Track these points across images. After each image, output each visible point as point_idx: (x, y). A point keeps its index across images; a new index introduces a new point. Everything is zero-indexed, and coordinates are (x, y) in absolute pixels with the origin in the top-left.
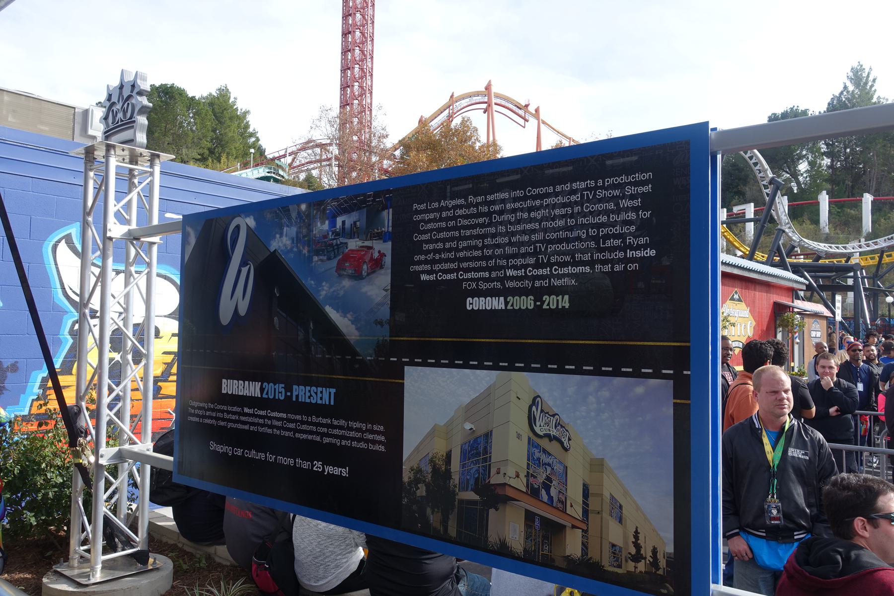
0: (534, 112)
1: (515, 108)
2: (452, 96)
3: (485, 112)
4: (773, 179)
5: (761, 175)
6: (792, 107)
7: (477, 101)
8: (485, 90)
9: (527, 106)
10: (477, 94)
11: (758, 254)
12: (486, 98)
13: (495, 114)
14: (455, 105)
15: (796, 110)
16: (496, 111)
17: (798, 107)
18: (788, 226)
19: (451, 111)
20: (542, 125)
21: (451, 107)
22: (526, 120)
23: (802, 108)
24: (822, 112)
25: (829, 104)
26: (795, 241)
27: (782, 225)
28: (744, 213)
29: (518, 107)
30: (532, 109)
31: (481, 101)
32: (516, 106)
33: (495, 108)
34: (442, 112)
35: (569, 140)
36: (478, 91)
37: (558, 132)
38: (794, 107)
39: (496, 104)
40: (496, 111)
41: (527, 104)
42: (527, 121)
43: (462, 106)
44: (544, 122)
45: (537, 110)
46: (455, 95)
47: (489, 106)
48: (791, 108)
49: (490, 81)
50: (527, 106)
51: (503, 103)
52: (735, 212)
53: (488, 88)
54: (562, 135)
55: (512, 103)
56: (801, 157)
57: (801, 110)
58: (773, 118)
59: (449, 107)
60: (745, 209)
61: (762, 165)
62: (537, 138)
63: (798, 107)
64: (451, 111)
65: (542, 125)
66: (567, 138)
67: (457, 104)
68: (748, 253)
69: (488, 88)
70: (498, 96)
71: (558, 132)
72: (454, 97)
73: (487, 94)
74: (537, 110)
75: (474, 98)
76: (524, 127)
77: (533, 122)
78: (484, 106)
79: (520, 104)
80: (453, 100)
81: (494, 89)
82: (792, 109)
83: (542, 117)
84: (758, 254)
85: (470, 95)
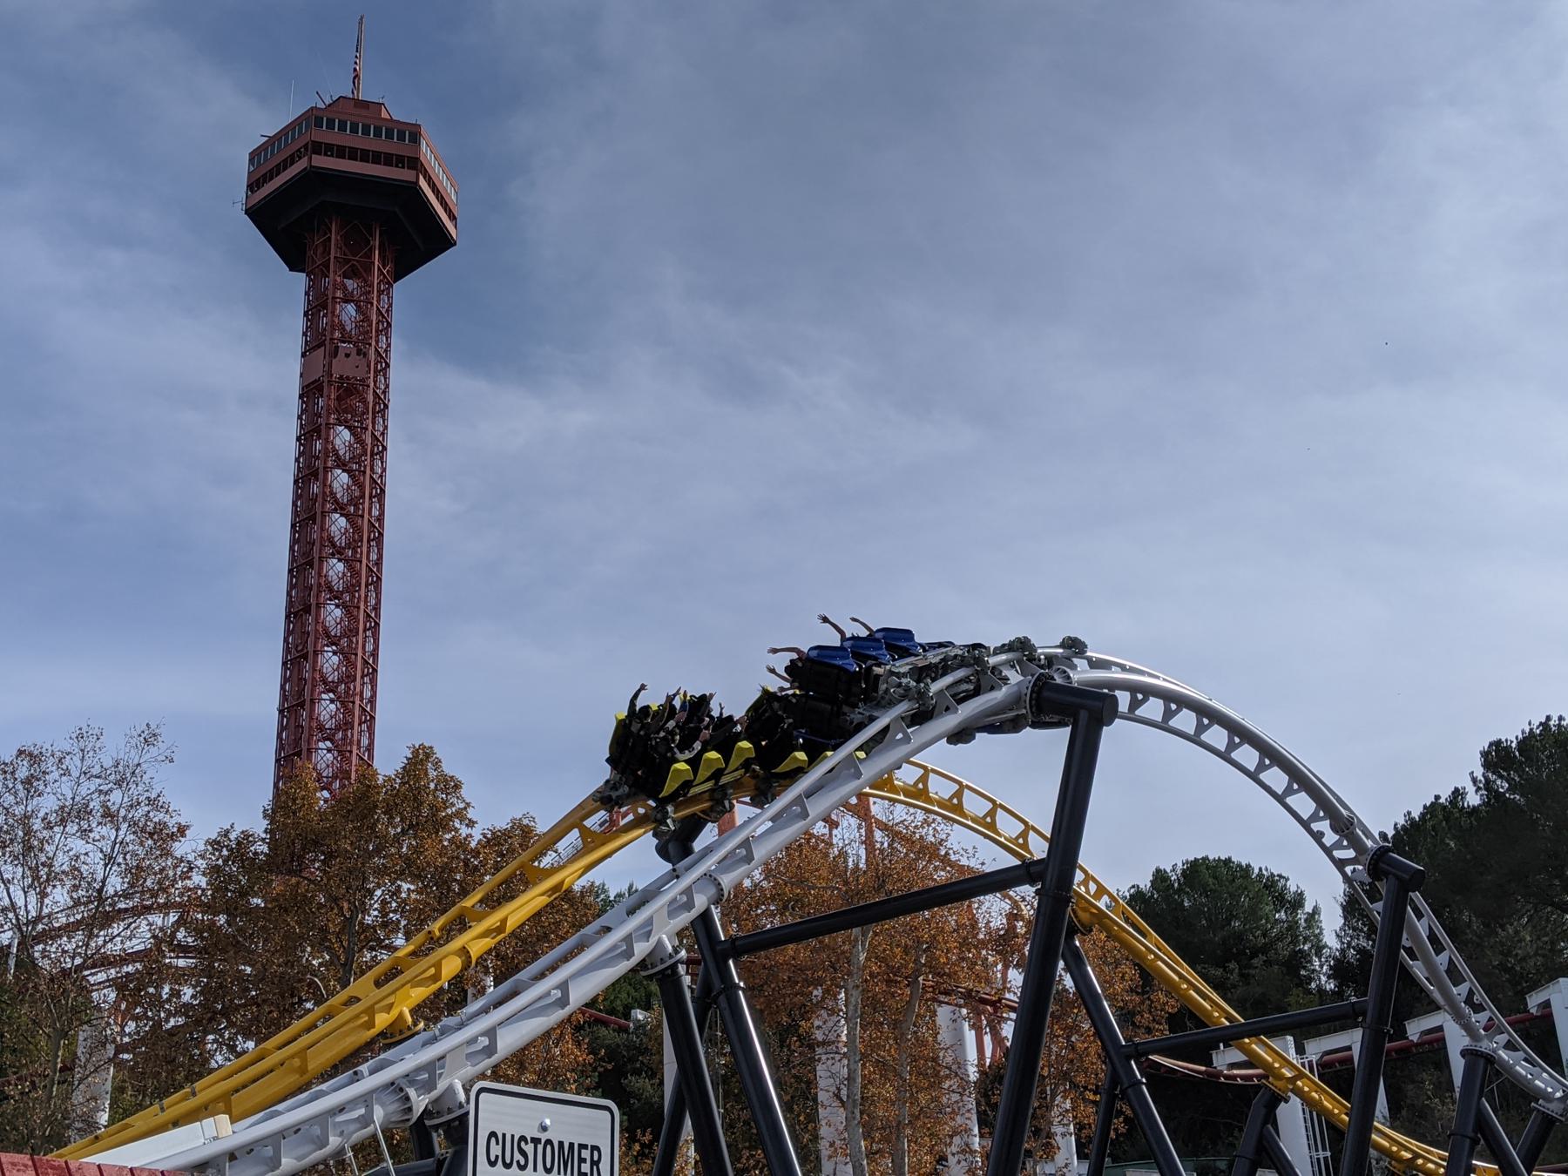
6: (1543, 720)
17: (1561, 718)
18: (1502, 1039)
26: (1548, 1098)
38: (1548, 718)
48: (1541, 724)
52: (1415, 1038)
58: (1497, 757)
63: (1561, 718)
82: (1545, 725)
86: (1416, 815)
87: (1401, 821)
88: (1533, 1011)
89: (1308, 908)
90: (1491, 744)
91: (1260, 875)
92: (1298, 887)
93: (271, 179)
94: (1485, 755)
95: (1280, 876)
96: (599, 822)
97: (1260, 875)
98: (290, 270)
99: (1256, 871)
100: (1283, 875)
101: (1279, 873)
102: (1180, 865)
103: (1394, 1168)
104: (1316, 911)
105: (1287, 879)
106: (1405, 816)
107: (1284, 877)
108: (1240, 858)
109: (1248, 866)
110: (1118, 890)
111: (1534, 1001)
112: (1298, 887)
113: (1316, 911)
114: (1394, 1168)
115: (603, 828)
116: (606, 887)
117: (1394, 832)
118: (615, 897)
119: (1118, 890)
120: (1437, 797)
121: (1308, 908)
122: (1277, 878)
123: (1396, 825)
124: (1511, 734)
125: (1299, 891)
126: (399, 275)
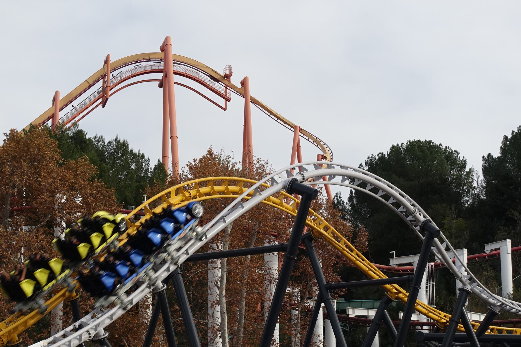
0: (240, 86)
1: (207, 80)
2: (107, 61)
5: (410, 218)
8: (160, 52)
9: (227, 76)
10: (148, 57)
12: (162, 63)
13: (176, 89)
14: (111, 75)
16: (175, 83)
20: (252, 107)
22: (227, 100)
26: (494, 305)
30: (236, 81)
31: (154, 68)
32: (210, 76)
34: (91, 86)
35: (293, 130)
36: (149, 54)
37: (278, 118)
39: (176, 73)
40: (175, 83)
41: (228, 72)
43: (123, 77)
44: (255, 102)
45: (244, 83)
46: (112, 60)
47: (166, 76)
49: (167, 39)
50: (227, 76)
55: (203, 72)
60: (499, 249)
62: (245, 126)
65: (252, 107)
66: (292, 127)
67: (115, 73)
69: (164, 48)
70: (178, 62)
71: (278, 118)
72: (111, 62)
73: (163, 57)
74: (244, 83)
76: (225, 109)
77: (237, 101)
79: (216, 73)
81: (175, 50)
83: (252, 92)
85: (136, 60)
89: (467, 170)
91: (446, 150)
92: (464, 158)
95: (456, 151)
96: (97, 91)
97: (446, 150)
99: (444, 148)
100: (457, 151)
101: (455, 149)
102: (405, 144)
103: (439, 325)
104: (471, 171)
105: (458, 153)
106: (518, 128)
107: (457, 152)
108: (436, 141)
109: (440, 145)
110: (372, 155)
112: (464, 158)
113: (471, 171)
114: (439, 325)
115: (99, 95)
116: (103, 138)
117: (511, 136)
118: (108, 144)
119: (372, 155)
121: (467, 170)
122: (454, 152)
123: (513, 132)
125: (464, 160)
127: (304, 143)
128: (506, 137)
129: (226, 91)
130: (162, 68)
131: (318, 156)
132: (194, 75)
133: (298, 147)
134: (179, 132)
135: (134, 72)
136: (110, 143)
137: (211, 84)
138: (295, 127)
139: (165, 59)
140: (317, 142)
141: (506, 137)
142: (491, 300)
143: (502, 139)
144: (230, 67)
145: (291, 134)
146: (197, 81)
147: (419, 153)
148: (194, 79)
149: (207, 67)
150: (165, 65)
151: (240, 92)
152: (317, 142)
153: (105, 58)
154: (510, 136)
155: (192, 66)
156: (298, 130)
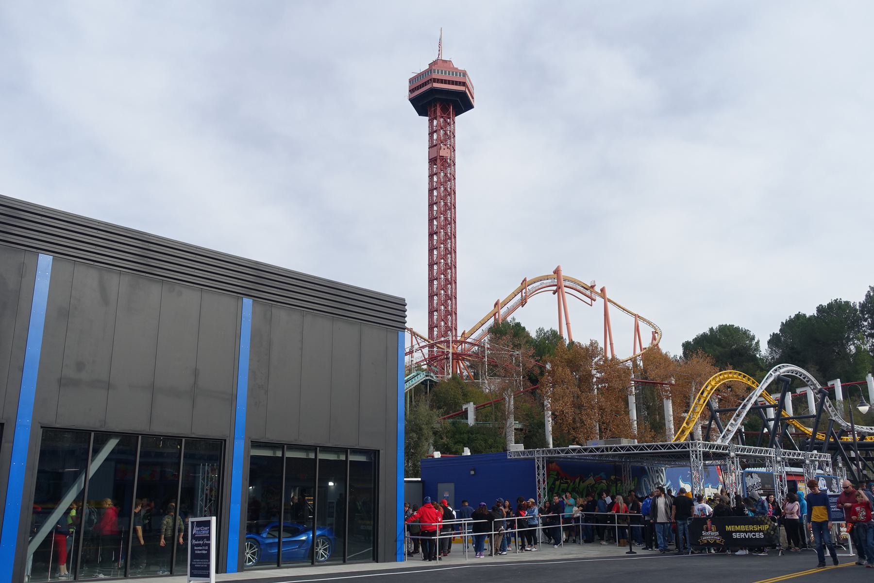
0: (600, 292)
1: (582, 289)
3: (554, 293)
4: (821, 389)
7: (548, 284)
9: (592, 287)
10: (547, 278)
11: (819, 435)
12: (556, 280)
15: (840, 301)
16: (566, 292)
17: (840, 299)
19: (524, 295)
20: (609, 304)
21: (524, 291)
23: (844, 300)
24: (862, 302)
25: (867, 296)
27: (832, 417)
28: (806, 393)
29: (584, 288)
30: (598, 289)
31: (551, 284)
32: (582, 287)
33: (566, 289)
34: (516, 295)
37: (624, 310)
38: (837, 299)
40: (566, 292)
41: (593, 284)
42: (595, 300)
44: (610, 301)
45: (602, 290)
48: (835, 300)
50: (592, 287)
51: (574, 286)
53: (557, 272)
54: (622, 309)
55: (578, 284)
56: (848, 339)
57: (844, 302)
58: (820, 309)
59: (521, 291)
61: (812, 381)
62: (605, 315)
63: (840, 299)
64: (524, 295)
65: (609, 304)
67: (530, 287)
68: (811, 434)
69: (557, 272)
71: (624, 310)
74: (602, 290)
75: (545, 281)
76: (591, 305)
77: (600, 301)
78: (555, 288)
79: (586, 285)
80: (525, 283)
81: (564, 273)
82: (836, 301)
83: (608, 296)
84: (819, 435)
86: (792, 317)
87: (788, 319)
88: (829, 386)
89: (756, 341)
90: (820, 305)
93: (418, 89)
94: (818, 308)
95: (748, 330)
98: (419, 115)
111: (830, 384)
113: (758, 342)
120: (799, 312)
124: (825, 303)
126: (456, 115)
127: (641, 324)
128: (782, 323)
129: (591, 295)
130: (556, 283)
131: (653, 332)
132: (571, 286)
133: (638, 326)
134: (570, 321)
135: (540, 287)
136: (548, 331)
137: (584, 292)
138: (635, 315)
139: (558, 278)
140: (649, 323)
141: (782, 323)
142: (843, 424)
143: (781, 324)
144: (594, 281)
145: (633, 319)
146: (576, 290)
147: (728, 333)
148: (574, 289)
149: (581, 282)
150: (558, 282)
151: (601, 295)
152: (649, 323)
153: (523, 279)
154: (784, 322)
155: (572, 282)
156: (636, 316)
